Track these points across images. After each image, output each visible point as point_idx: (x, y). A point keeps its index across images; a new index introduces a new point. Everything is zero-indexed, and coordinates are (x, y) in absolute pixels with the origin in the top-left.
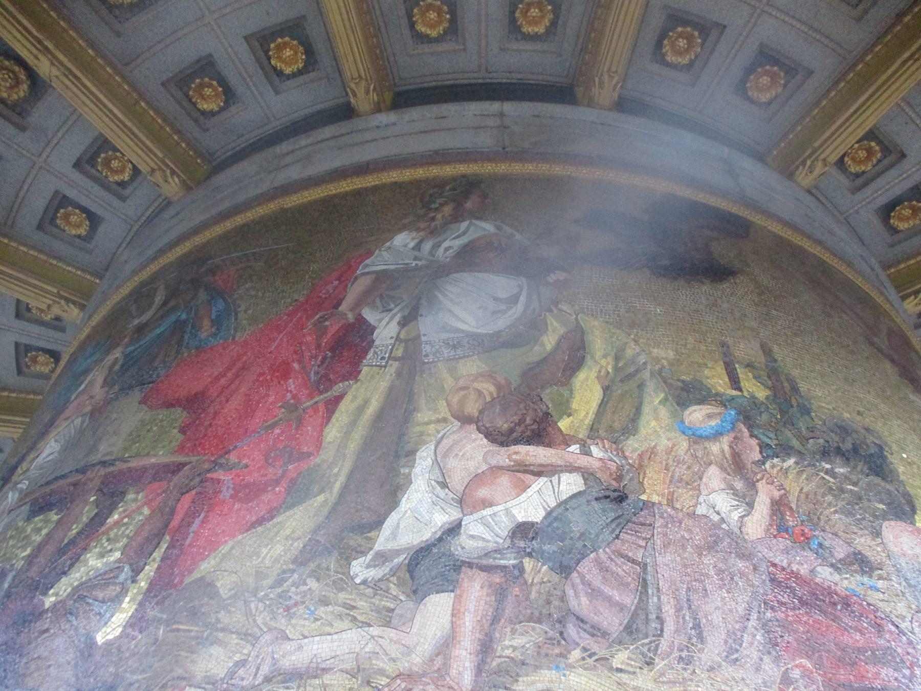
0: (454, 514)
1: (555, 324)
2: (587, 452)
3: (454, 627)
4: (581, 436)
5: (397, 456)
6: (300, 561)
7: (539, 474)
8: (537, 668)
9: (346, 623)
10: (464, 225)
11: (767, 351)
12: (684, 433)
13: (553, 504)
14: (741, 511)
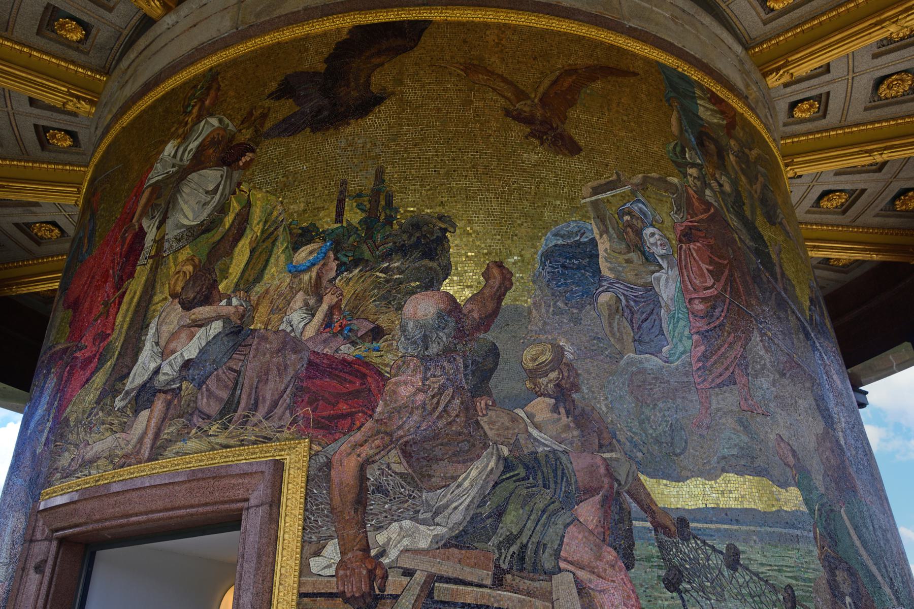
0: (159, 361)
1: (235, 204)
2: (229, 303)
3: (146, 429)
4: (229, 293)
5: (142, 329)
6: (98, 402)
7: (200, 326)
8: (176, 441)
10: (203, 122)
11: (380, 175)
12: (290, 272)
13: (204, 344)
14: (306, 320)
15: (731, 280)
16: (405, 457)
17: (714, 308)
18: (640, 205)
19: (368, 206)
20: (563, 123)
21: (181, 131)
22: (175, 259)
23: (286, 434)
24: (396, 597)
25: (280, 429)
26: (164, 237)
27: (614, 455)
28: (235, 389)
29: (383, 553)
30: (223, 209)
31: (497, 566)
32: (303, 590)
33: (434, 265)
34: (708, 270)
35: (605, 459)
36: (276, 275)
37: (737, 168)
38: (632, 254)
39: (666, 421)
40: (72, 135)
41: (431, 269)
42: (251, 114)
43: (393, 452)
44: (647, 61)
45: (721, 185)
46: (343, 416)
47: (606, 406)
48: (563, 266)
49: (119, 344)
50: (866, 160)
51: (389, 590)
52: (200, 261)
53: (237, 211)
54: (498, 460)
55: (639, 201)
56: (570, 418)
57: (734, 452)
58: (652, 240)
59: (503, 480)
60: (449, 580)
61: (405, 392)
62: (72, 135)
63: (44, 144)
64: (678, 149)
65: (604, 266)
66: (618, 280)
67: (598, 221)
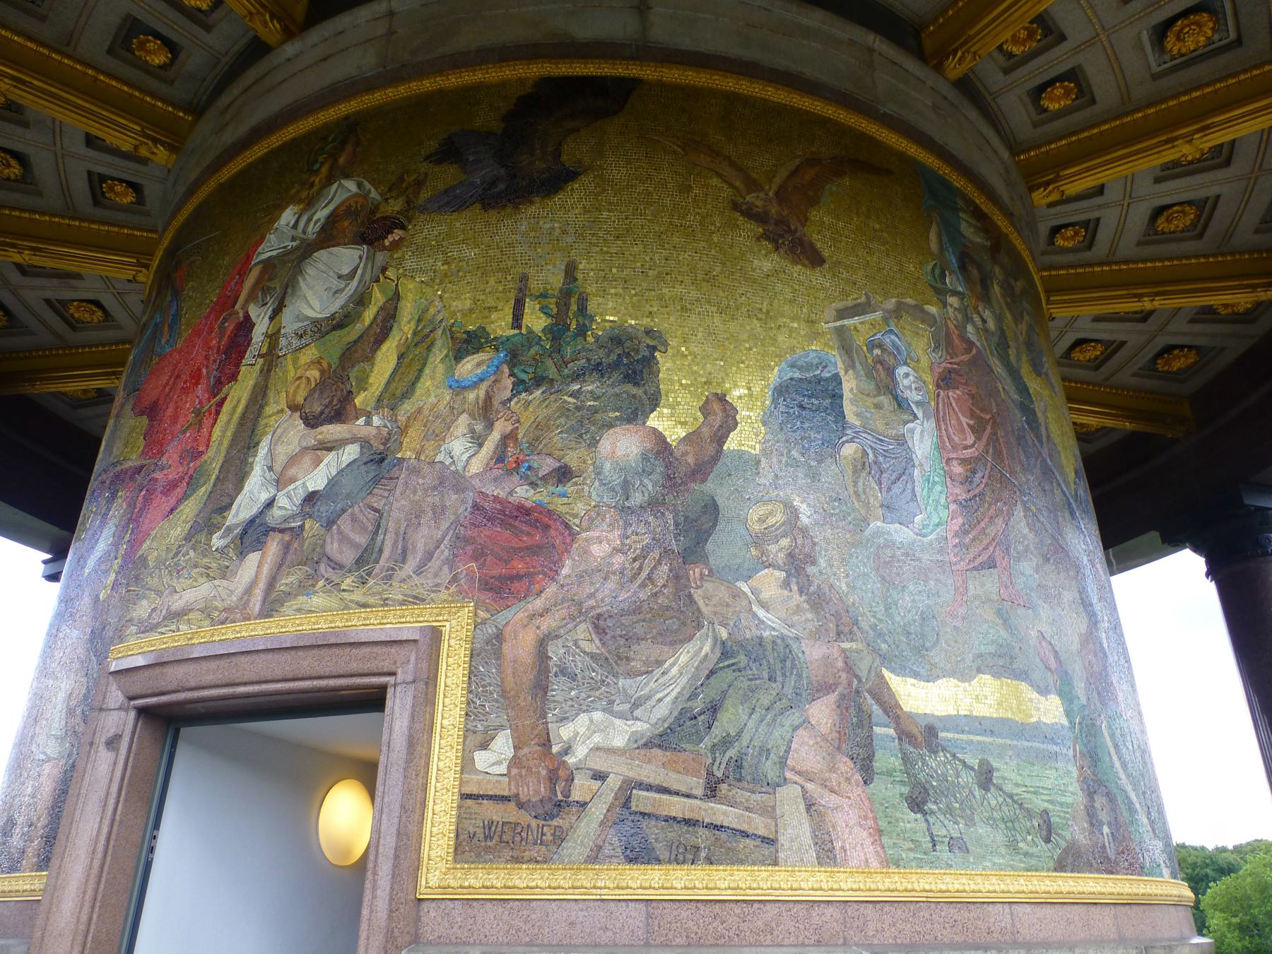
1: (378, 295)
2: (368, 423)
4: (369, 409)
6: (188, 538)
7: (330, 449)
8: (297, 595)
9: (205, 579)
10: (336, 185)
13: (334, 472)
14: (471, 452)
15: (994, 439)
16: (598, 633)
17: (974, 472)
18: (893, 337)
19: (555, 310)
20: (803, 226)
21: (304, 195)
22: (295, 361)
23: (444, 595)
24: (583, 805)
25: (436, 588)
26: (279, 330)
27: (854, 645)
28: (376, 533)
29: (567, 750)
30: (361, 300)
31: (710, 773)
32: (467, 790)
33: (639, 392)
35: (844, 651)
36: (431, 390)
37: (1002, 302)
38: (882, 398)
40: (135, 187)
41: (634, 396)
42: (401, 179)
43: (583, 626)
44: (903, 158)
45: (984, 321)
46: (519, 577)
47: (848, 585)
48: (801, 407)
49: (216, 466)
50: (1132, 306)
51: (576, 796)
52: (330, 366)
53: (380, 304)
54: (715, 644)
56: (804, 598)
57: (992, 649)
58: (906, 382)
59: (721, 669)
60: (649, 788)
61: (598, 550)
62: (135, 187)
63: (97, 198)
64: (937, 271)
65: (849, 409)
66: (865, 428)
67: (843, 352)
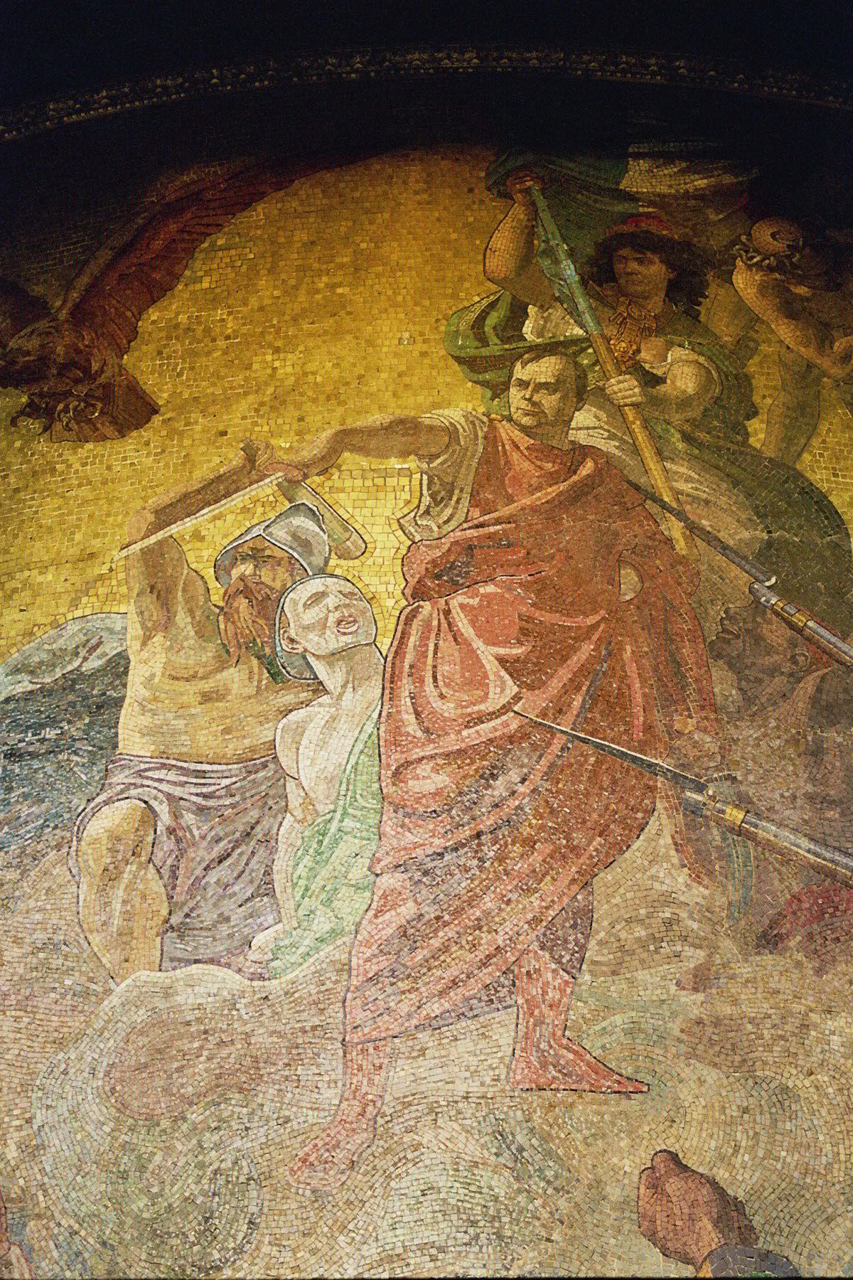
20: (121, 352)
34: (502, 661)
39: (201, 1166)
55: (297, 509)
67: (149, 600)
